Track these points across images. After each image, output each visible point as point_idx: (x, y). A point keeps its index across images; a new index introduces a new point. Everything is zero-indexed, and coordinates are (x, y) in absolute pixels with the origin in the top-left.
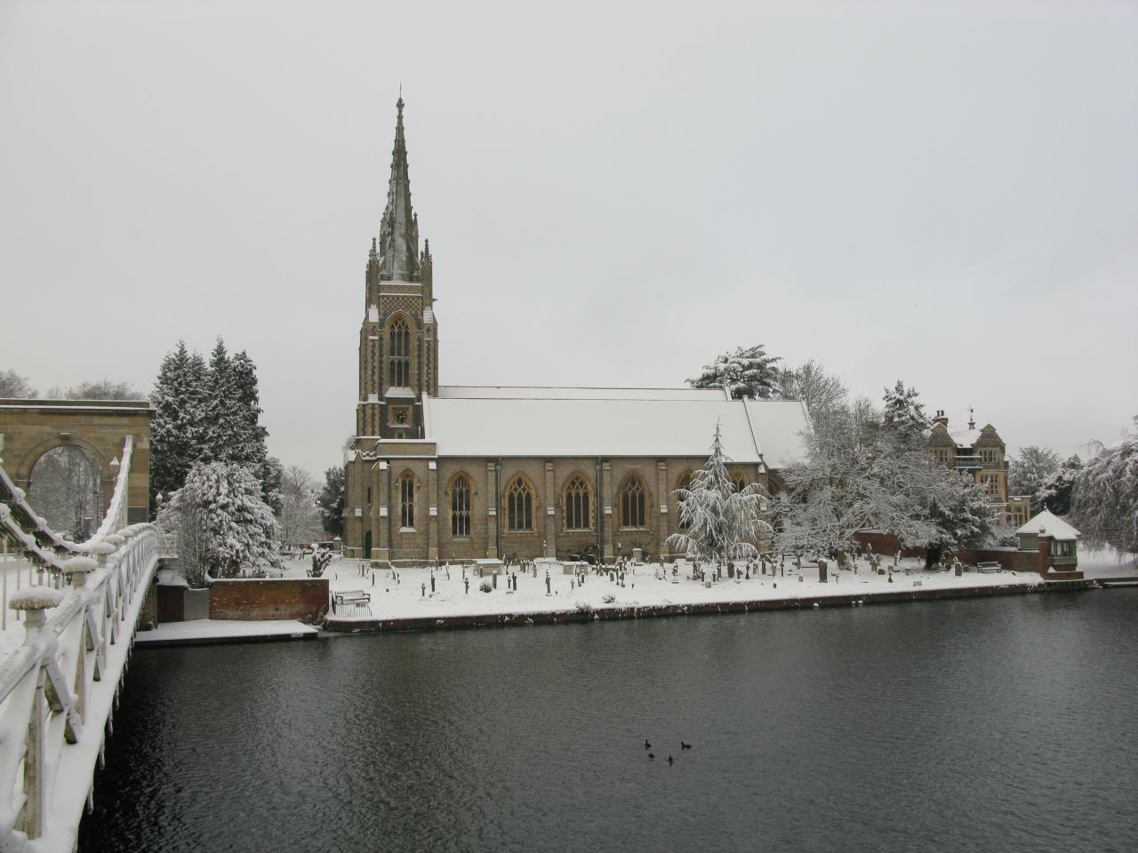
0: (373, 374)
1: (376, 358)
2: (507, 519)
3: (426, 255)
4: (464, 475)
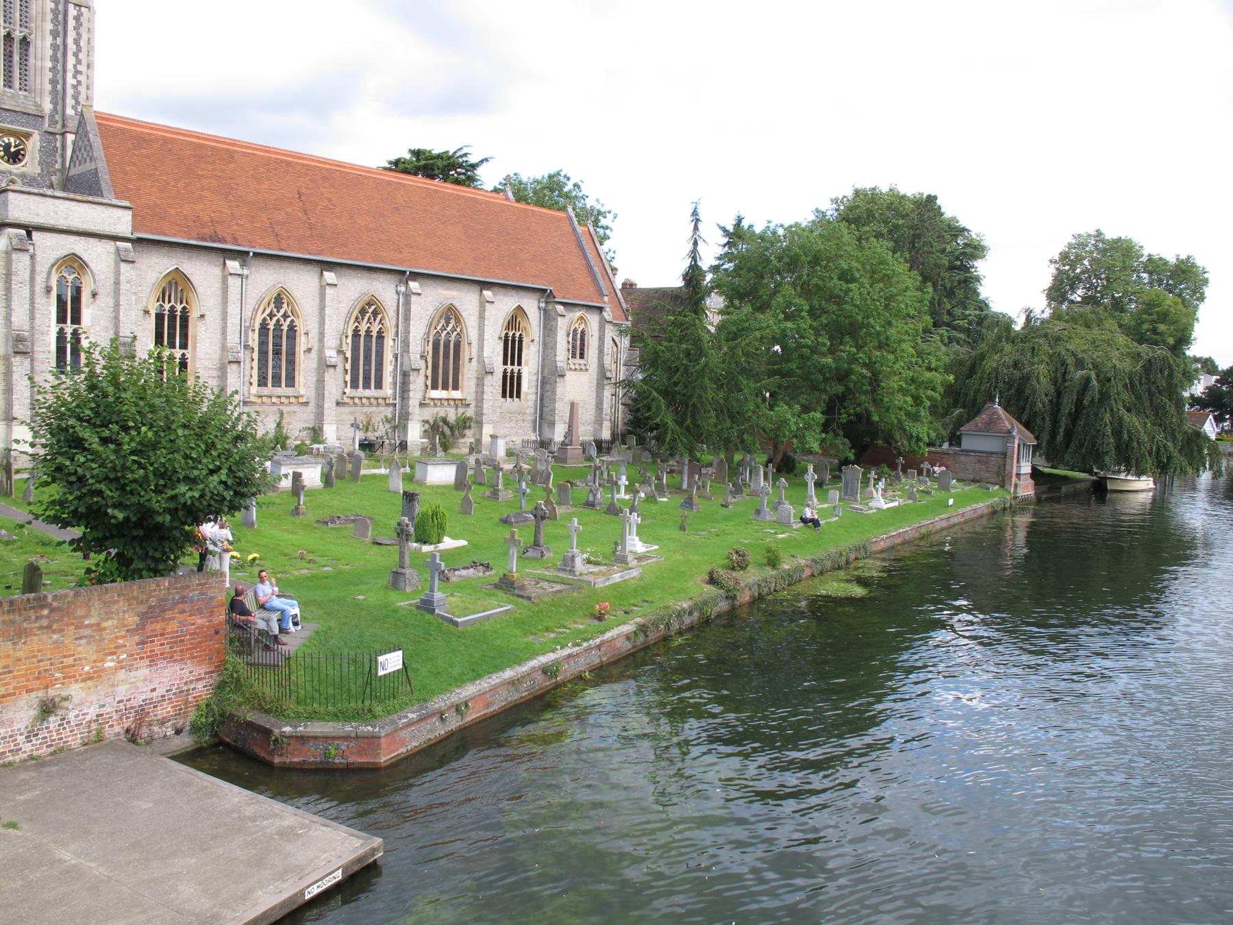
4: (178, 277)
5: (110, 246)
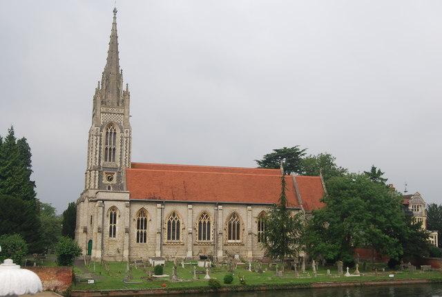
0: (96, 154)
1: (98, 146)
2: (166, 233)
3: (127, 94)
5: (124, 203)
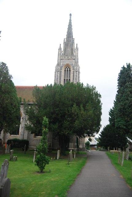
3: (77, 49)
